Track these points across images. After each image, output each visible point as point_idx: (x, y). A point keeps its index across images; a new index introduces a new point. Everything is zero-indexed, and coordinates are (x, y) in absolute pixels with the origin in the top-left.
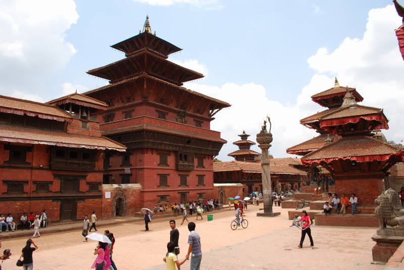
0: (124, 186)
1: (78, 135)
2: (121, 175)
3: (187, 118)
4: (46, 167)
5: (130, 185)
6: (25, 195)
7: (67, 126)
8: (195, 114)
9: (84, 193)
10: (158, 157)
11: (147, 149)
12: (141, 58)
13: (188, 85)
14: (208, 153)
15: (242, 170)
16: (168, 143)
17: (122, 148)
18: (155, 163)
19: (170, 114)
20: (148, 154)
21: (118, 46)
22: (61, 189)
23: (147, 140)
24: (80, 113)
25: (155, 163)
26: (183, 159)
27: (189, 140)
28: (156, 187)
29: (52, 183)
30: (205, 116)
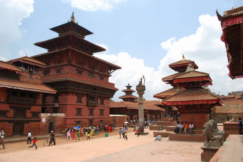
0: (54, 115)
1: (27, 82)
2: (52, 108)
3: (95, 75)
4: (5, 102)
5: (58, 114)
7: (20, 76)
8: (99, 72)
9: (29, 118)
10: (76, 97)
11: (70, 92)
12: (68, 37)
13: (96, 55)
14: (107, 96)
15: (127, 107)
17: (54, 91)
18: (74, 101)
19: (85, 72)
21: (55, 29)
23: (69, 87)
24: (29, 68)
25: (74, 101)
27: (95, 88)
28: (74, 116)
29: (8, 111)
30: (106, 74)
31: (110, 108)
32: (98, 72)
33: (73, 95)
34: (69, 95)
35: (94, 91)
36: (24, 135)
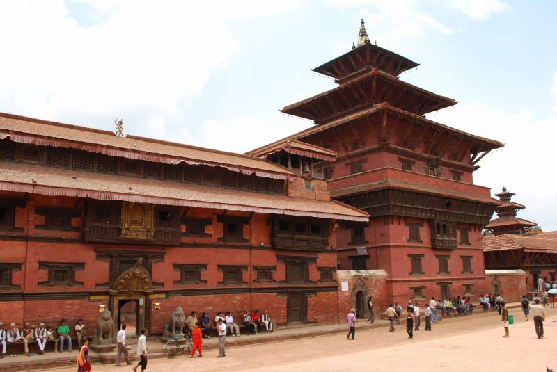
0: (364, 273)
1: (302, 198)
5: (371, 272)
6: (245, 286)
7: (287, 187)
9: (315, 282)
11: (393, 216)
12: (366, 84)
15: (524, 248)
16: (420, 207)
17: (359, 214)
20: (394, 225)
21: (325, 69)
22: (286, 278)
23: (392, 203)
25: (404, 238)
26: (441, 231)
27: (448, 202)
28: (407, 274)
29: (275, 268)
30: (464, 163)
31: (484, 252)
32: (447, 161)
33: (399, 224)
34: (392, 224)
35: (445, 210)
36: (310, 322)
